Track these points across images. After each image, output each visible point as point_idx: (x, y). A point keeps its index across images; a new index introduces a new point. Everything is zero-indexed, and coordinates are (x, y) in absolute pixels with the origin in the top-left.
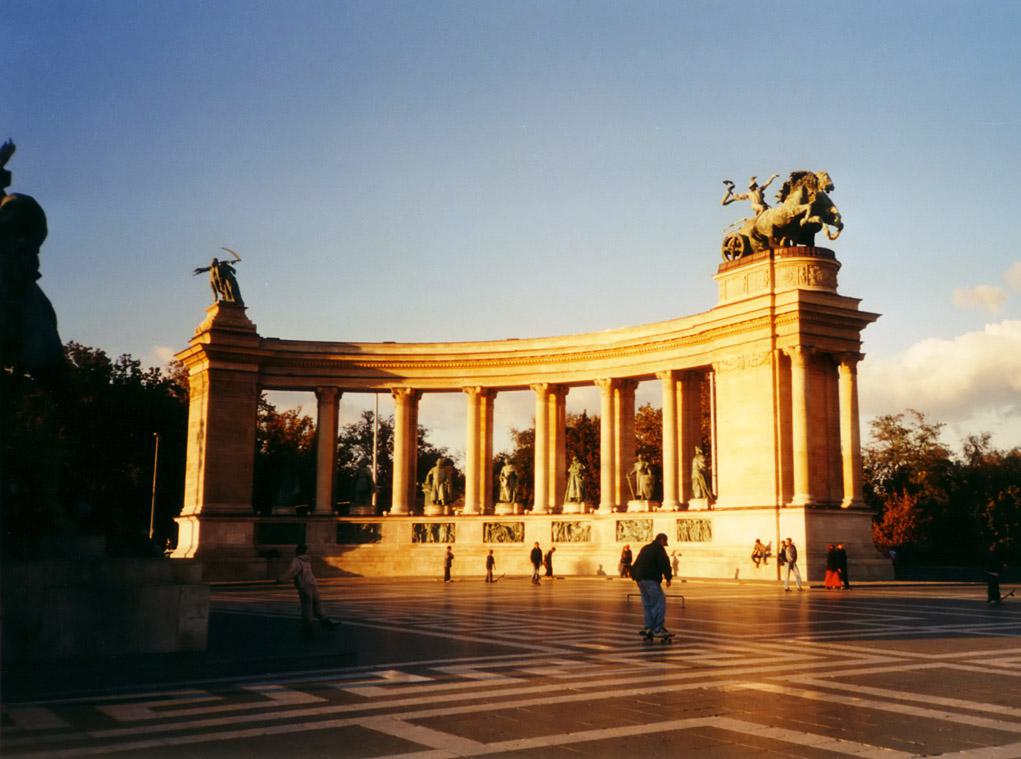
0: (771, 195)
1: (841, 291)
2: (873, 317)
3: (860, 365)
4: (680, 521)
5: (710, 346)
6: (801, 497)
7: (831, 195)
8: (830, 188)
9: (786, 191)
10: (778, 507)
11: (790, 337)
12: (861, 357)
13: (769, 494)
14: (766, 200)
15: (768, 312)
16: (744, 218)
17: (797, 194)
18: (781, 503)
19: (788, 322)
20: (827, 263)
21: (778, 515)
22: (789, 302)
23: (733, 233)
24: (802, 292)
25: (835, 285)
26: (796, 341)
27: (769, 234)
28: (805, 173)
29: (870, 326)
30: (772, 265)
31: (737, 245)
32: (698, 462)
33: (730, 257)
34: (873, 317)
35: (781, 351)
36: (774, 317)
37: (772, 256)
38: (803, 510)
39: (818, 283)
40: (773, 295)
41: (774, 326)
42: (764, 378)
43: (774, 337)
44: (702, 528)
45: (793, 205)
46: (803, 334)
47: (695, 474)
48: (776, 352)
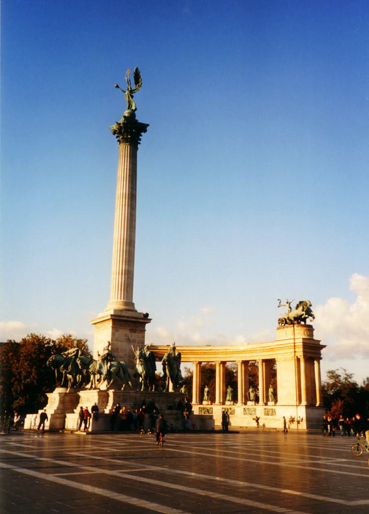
0: (294, 306)
1: (315, 338)
2: (324, 346)
3: (321, 361)
4: (265, 409)
5: (274, 353)
6: (304, 403)
7: (311, 308)
8: (311, 305)
9: (297, 307)
10: (297, 406)
11: (300, 353)
12: (321, 359)
13: (294, 401)
14: (291, 306)
15: (293, 345)
16: (284, 313)
17: (301, 308)
18: (298, 404)
19: (299, 348)
20: (310, 329)
21: (297, 408)
22: (299, 342)
23: (281, 317)
24: (303, 339)
25: (313, 336)
26: (301, 354)
27: (293, 319)
28: (303, 302)
29: (324, 349)
30: (294, 329)
31: (283, 321)
32: (271, 390)
33: (280, 324)
34: (324, 346)
35: (297, 357)
36: (295, 346)
37: (294, 327)
38: (304, 407)
39: (308, 336)
40: (294, 339)
41: (295, 349)
42: (293, 364)
43: (295, 352)
44: (272, 411)
45: (300, 311)
46: (304, 352)
47: (270, 394)
48: (296, 357)
